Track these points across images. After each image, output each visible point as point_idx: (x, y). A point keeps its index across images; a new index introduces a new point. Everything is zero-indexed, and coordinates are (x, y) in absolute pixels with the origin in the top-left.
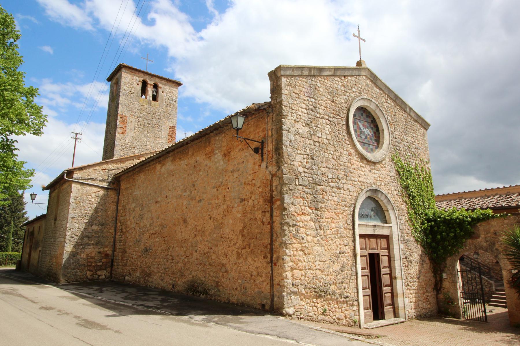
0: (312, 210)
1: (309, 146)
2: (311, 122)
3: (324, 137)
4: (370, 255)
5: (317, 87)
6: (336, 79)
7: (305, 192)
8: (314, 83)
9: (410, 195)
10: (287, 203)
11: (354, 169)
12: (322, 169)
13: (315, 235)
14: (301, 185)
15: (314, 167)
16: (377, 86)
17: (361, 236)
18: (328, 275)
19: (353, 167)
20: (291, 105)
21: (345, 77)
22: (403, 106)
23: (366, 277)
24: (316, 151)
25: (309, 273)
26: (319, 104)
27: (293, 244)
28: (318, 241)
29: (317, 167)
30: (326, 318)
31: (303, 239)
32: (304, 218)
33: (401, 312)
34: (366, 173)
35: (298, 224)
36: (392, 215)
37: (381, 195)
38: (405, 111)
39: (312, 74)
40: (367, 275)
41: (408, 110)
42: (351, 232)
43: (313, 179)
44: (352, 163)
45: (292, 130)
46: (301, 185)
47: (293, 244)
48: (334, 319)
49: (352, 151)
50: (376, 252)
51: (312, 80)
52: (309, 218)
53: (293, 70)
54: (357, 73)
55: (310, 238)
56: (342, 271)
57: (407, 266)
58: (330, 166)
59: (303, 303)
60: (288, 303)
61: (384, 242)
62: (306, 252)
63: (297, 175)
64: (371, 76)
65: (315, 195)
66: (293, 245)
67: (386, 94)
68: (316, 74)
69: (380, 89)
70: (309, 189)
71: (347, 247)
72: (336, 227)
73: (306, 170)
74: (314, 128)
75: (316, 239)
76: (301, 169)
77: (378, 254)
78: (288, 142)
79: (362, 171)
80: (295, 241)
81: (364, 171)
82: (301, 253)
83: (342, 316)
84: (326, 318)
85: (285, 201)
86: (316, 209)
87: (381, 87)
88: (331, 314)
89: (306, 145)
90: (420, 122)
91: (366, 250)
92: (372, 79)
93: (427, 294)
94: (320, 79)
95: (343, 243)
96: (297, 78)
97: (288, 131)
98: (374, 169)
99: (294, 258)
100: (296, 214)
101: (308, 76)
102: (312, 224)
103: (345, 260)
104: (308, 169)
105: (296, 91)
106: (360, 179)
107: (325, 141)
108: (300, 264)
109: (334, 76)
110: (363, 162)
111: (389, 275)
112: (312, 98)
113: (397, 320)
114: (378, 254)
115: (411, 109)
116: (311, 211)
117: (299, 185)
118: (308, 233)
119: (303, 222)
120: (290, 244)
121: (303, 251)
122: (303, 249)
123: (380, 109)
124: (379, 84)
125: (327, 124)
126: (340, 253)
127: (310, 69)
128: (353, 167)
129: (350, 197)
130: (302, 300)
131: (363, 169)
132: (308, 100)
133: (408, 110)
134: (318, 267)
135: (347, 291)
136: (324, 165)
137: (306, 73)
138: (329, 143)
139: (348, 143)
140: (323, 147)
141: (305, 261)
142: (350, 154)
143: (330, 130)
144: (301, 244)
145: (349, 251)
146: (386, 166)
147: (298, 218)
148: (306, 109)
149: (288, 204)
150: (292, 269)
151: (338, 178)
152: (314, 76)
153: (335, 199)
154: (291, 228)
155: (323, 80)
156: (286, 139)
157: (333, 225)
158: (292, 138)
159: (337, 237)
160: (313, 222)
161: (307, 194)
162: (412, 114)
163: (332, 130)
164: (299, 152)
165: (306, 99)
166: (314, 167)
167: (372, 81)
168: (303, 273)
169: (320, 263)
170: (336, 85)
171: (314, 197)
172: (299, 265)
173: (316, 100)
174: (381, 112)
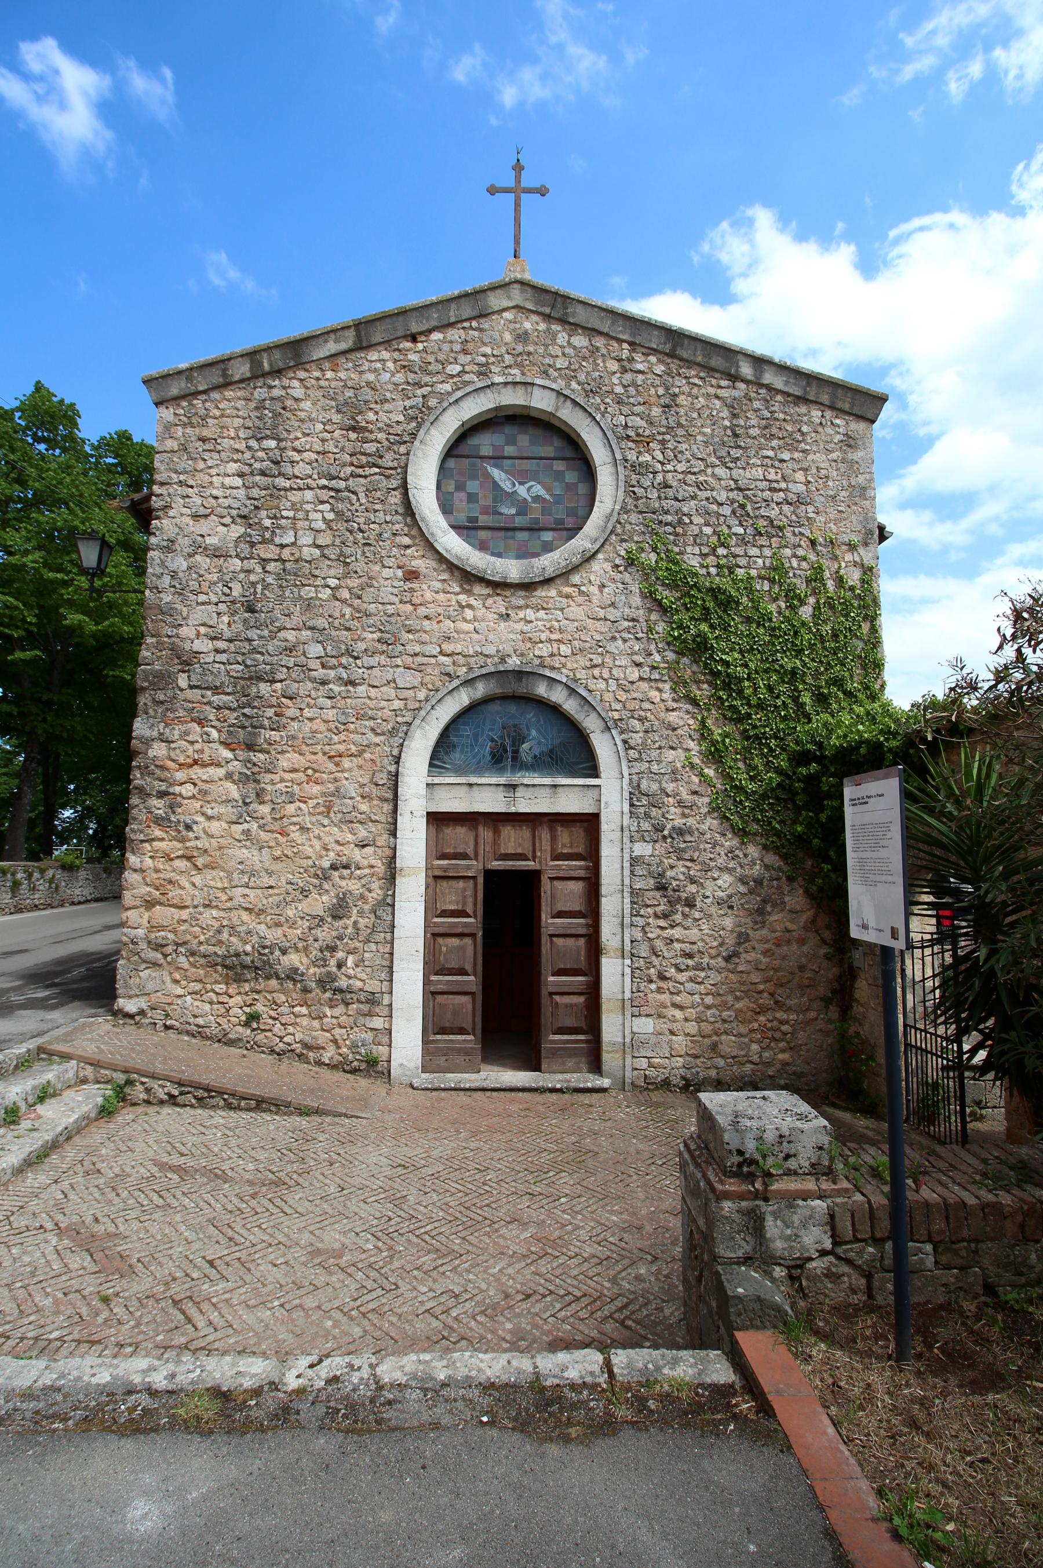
0: (233, 750)
1: (242, 576)
2: (257, 508)
3: (306, 539)
4: (489, 874)
5: (289, 403)
6: (373, 355)
7: (209, 703)
8: (276, 393)
9: (716, 674)
10: (140, 738)
11: (427, 617)
12: (282, 634)
13: (234, 818)
14: (197, 687)
15: (253, 634)
16: (574, 327)
17: (436, 819)
18: (278, 925)
19: (422, 611)
20: (182, 477)
21: (414, 339)
22: (716, 362)
23: (468, 941)
25: (208, 917)
26: (294, 449)
27: (153, 840)
28: (247, 833)
29: (266, 633)
30: (260, 1037)
31: (188, 828)
32: (197, 772)
33: (610, 1059)
34: (482, 626)
35: (177, 789)
36: (603, 747)
37: (550, 687)
38: (735, 378)
39: (266, 366)
40: (473, 935)
41: (746, 370)
42: (387, 807)
43: (246, 666)
44: (415, 601)
45: (183, 542)
46: (197, 687)
47: (153, 840)
48: (289, 1044)
49: (422, 564)
50: (530, 865)
51: (271, 387)
52: (221, 772)
53: (189, 379)
54: (467, 311)
55: (215, 827)
56: (336, 917)
57: (665, 916)
58: (321, 623)
59: (179, 991)
60: (127, 986)
61: (568, 839)
62: (200, 862)
63: (186, 661)
64: (537, 303)
65: (246, 711)
66: (155, 844)
67: (620, 341)
68: (281, 365)
69: (592, 332)
70: (228, 694)
71: (369, 850)
72: (324, 794)
73: (221, 645)
74: (267, 523)
75: (238, 828)
76: (202, 645)
77: (533, 877)
78: (167, 579)
79: (465, 620)
80: (158, 833)
81: (475, 619)
83: (323, 1038)
84: (260, 1037)
85: (134, 734)
86: (250, 747)
87: (595, 322)
88: (278, 1028)
89: (227, 578)
90: (825, 398)
91: (476, 859)
92: (547, 310)
93: (779, 1015)
94: (302, 374)
95: (350, 837)
96: (215, 395)
97: (169, 547)
98: (527, 607)
99: (155, 876)
100: (170, 764)
101: (254, 377)
103: (354, 886)
104: (230, 641)
105: (206, 433)
106: (448, 648)
107: (308, 552)
108: (174, 893)
109: (361, 346)
110: (469, 593)
111: (582, 941)
112: (267, 437)
113: (593, 1081)
115: (760, 362)
116: (229, 755)
117: (191, 687)
118: (210, 812)
119: (195, 785)
120: (142, 841)
121: (189, 858)
122: (189, 853)
123: (575, 403)
124: (580, 315)
125: (322, 502)
126: (334, 867)
127: (252, 355)
128: (422, 611)
129: (397, 704)
130: (176, 982)
131: (469, 614)
132: (249, 448)
133: (746, 370)
134: (239, 900)
135: (351, 972)
136: (296, 620)
137: (242, 369)
138: (324, 556)
139: (407, 541)
140: (293, 573)
141: (191, 886)
142: (412, 575)
143: (331, 516)
144: (183, 840)
145: (379, 863)
146: (594, 589)
147: (180, 776)
148: (241, 475)
149: (148, 742)
150: (150, 904)
151: (349, 652)
152: (278, 373)
153: (330, 714)
154: (155, 802)
155: (317, 374)
156: (158, 570)
157: (316, 789)
158: (180, 563)
159: (326, 822)
160: (234, 782)
161: (219, 708)
162: (768, 378)
163: (339, 514)
164: (202, 598)
165: (241, 446)
166: (253, 634)
167: (547, 317)
168: (185, 914)
169: (247, 891)
170: (371, 377)
171: (244, 715)
172: (170, 894)
173: (280, 440)
174: (580, 414)
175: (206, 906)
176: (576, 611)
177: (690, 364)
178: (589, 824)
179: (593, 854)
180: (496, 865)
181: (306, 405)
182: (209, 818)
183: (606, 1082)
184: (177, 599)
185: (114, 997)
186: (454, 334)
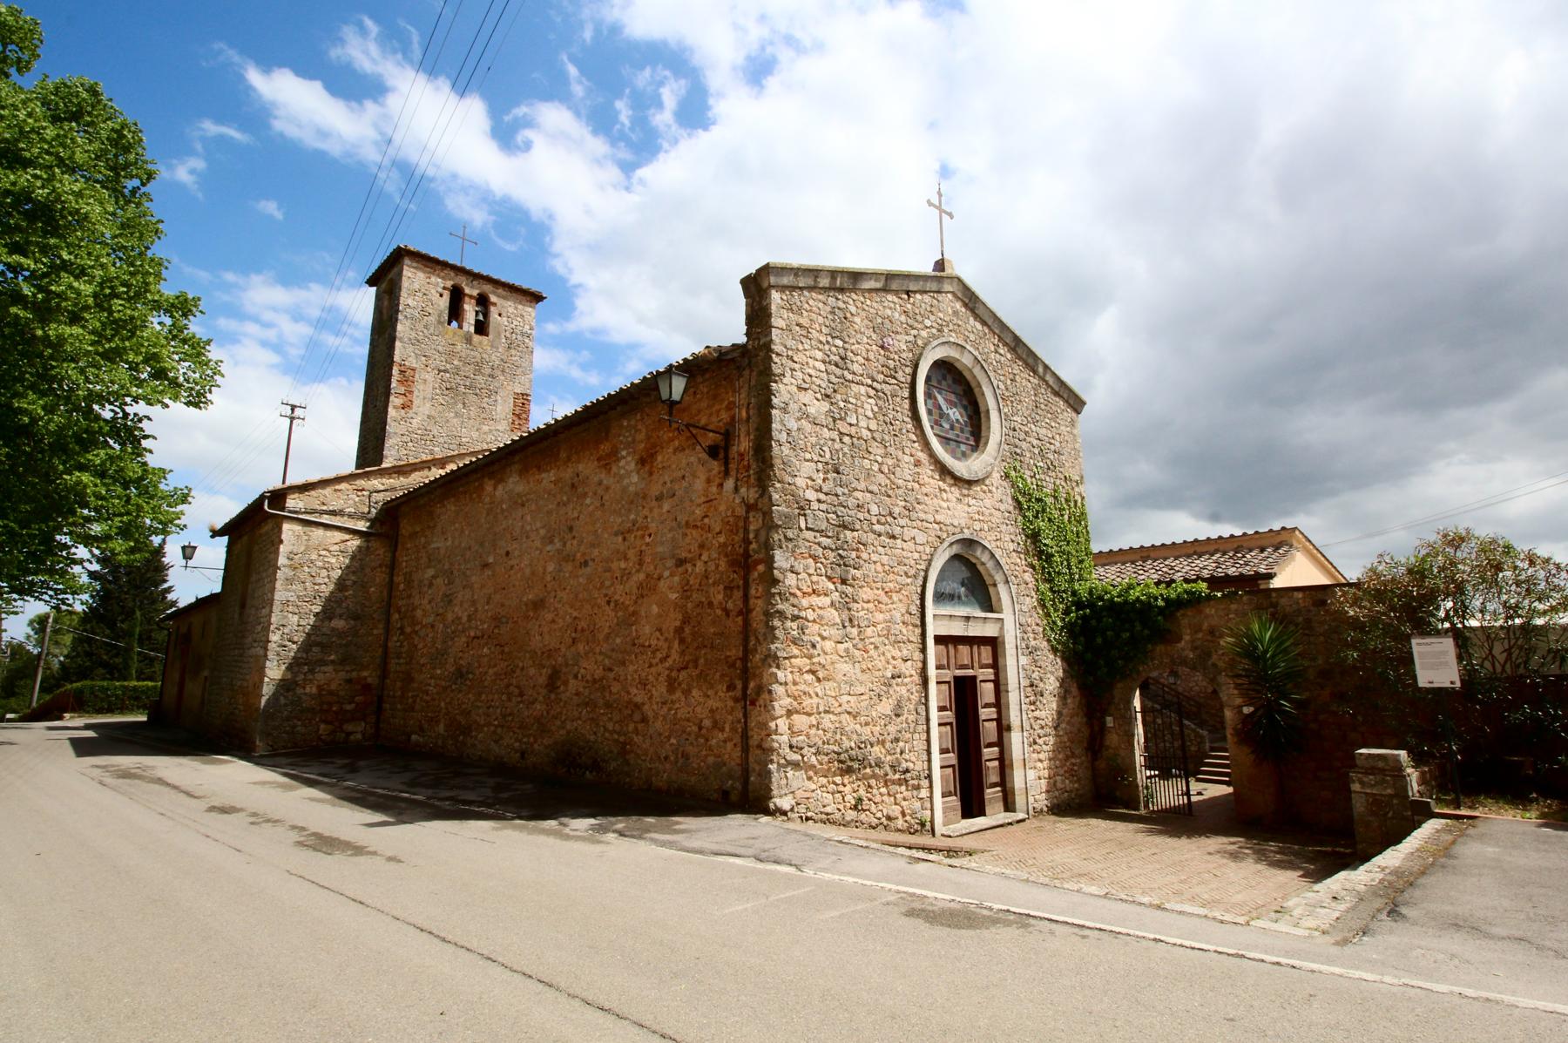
3: (863, 424)
4: (956, 678)
6: (890, 297)
7: (819, 544)
9: (1041, 552)
10: (779, 569)
12: (856, 494)
15: (839, 490)
16: (977, 317)
17: (939, 640)
18: (867, 724)
19: (924, 490)
21: (908, 293)
22: (1030, 361)
24: (844, 455)
25: (827, 721)
28: (847, 650)
31: (814, 646)
32: (815, 600)
33: (1020, 800)
35: (803, 614)
38: (1035, 372)
41: (1041, 370)
42: (918, 631)
45: (793, 407)
49: (923, 456)
50: (970, 672)
52: (826, 601)
53: (796, 275)
54: (934, 286)
55: (828, 645)
56: (898, 715)
57: (1033, 703)
58: (875, 488)
59: (814, 787)
60: (780, 787)
61: (986, 653)
62: (821, 675)
63: (803, 508)
69: (984, 323)
73: (822, 497)
74: (842, 404)
76: (811, 495)
77: (974, 678)
80: (796, 652)
82: (809, 677)
83: (895, 811)
84: (863, 817)
86: (844, 582)
88: (873, 808)
97: (785, 410)
101: (830, 289)
102: (833, 615)
103: (903, 691)
106: (939, 518)
107: (865, 434)
108: (807, 702)
109: (885, 290)
110: (944, 481)
113: (1011, 817)
114: (974, 678)
115: (1046, 367)
116: (831, 586)
121: (813, 672)
124: (980, 311)
127: (833, 273)
128: (924, 490)
129: (916, 556)
130: (810, 778)
133: (1041, 370)
134: (845, 706)
136: (862, 486)
137: (824, 282)
140: (859, 447)
141: (817, 695)
142: (917, 464)
144: (810, 657)
147: (805, 602)
150: (789, 713)
151: (891, 514)
152: (842, 290)
153: (885, 559)
154: (789, 624)
157: (880, 617)
158: (793, 425)
162: (1048, 378)
163: (880, 408)
164: (808, 456)
165: (823, 339)
166: (839, 490)
167: (965, 305)
168: (813, 720)
170: (889, 312)
175: (826, 712)
176: (988, 502)
177: (1020, 358)
178: (994, 643)
179: (996, 665)
180: (959, 673)
181: (857, 320)
182: (823, 638)
183: (1021, 816)
184: (792, 453)
185: (767, 795)
186: (927, 298)
